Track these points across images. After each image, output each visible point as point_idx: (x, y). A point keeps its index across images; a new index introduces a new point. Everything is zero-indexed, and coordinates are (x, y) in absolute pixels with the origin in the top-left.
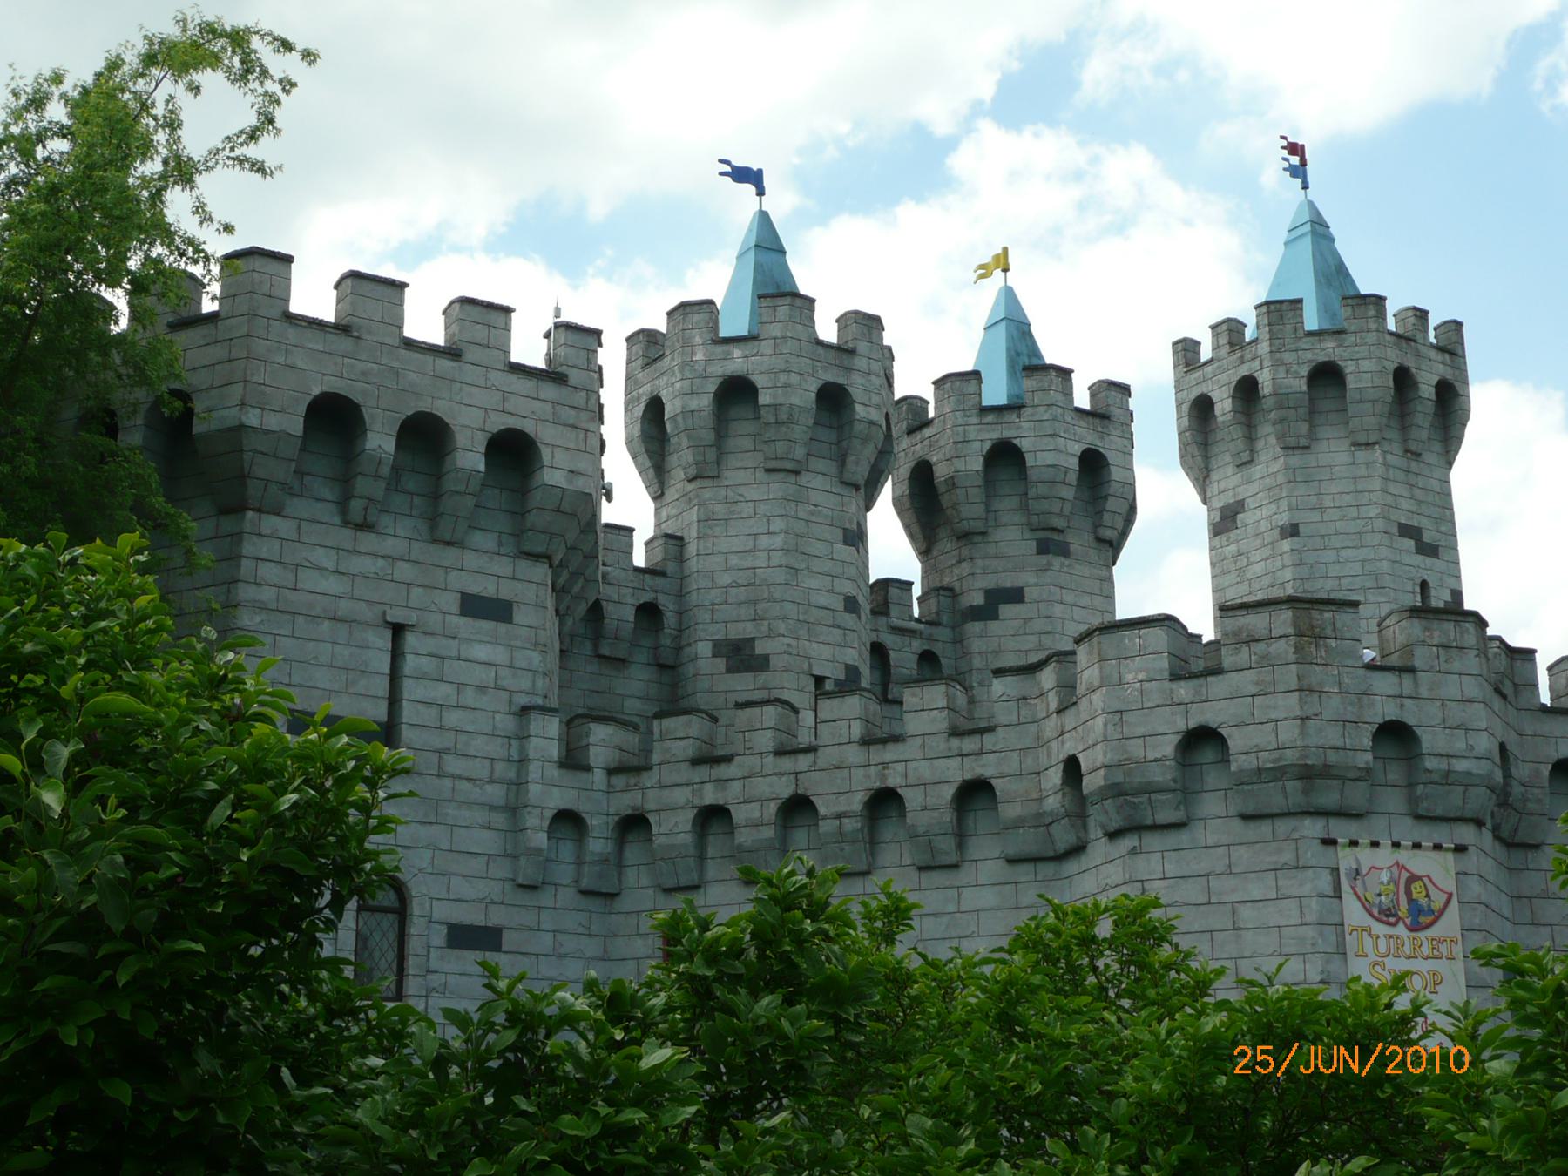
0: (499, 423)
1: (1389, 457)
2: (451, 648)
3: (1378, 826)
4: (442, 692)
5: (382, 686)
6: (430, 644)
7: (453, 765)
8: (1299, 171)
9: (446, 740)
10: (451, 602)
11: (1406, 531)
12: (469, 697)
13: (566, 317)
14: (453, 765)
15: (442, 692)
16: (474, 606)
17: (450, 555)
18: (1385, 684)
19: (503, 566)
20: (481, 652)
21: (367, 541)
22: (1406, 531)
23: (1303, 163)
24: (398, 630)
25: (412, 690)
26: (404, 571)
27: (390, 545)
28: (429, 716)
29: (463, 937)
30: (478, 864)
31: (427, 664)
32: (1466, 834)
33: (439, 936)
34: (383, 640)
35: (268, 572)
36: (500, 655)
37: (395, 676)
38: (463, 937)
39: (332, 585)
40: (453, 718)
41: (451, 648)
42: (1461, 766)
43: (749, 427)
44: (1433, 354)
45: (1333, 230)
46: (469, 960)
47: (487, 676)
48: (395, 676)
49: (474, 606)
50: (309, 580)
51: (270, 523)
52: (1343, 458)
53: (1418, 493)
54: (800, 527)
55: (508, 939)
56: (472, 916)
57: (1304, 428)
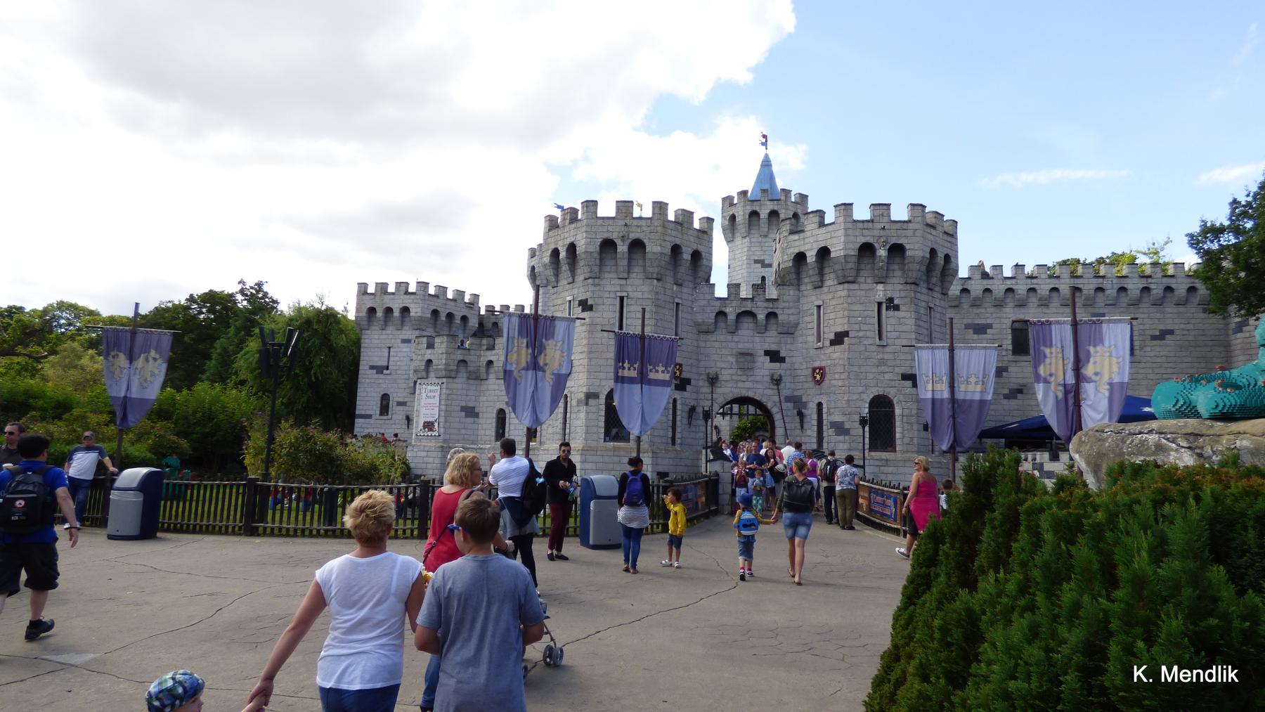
0: (402, 306)
1: (753, 240)
2: (399, 350)
3: (429, 381)
4: (397, 358)
5: (386, 359)
6: (395, 350)
7: (399, 372)
8: (764, 144)
9: (397, 368)
10: (399, 341)
11: (756, 262)
12: (402, 359)
13: (419, 280)
14: (399, 372)
15: (397, 358)
16: (404, 341)
17: (399, 332)
18: (429, 351)
19: (410, 332)
20: (404, 350)
21: (384, 332)
22: (756, 262)
23: (766, 141)
24: (390, 348)
25: (391, 359)
26: (391, 337)
27: (388, 332)
28: (394, 363)
29: (399, 404)
30: (403, 390)
31: (395, 354)
32: (444, 380)
33: (395, 404)
34: (387, 350)
35: (367, 341)
36: (408, 350)
37: (389, 356)
38: (399, 404)
39: (377, 341)
40: (398, 363)
41: (399, 350)
42: (439, 367)
43: (613, 262)
44: (672, 226)
45: (772, 163)
46: (401, 408)
47: (405, 354)
48: (389, 356)
49: (404, 341)
50: (374, 341)
51: (367, 332)
52: (740, 242)
53: (764, 248)
54: (546, 299)
55: (408, 404)
56: (401, 400)
57: (730, 235)
